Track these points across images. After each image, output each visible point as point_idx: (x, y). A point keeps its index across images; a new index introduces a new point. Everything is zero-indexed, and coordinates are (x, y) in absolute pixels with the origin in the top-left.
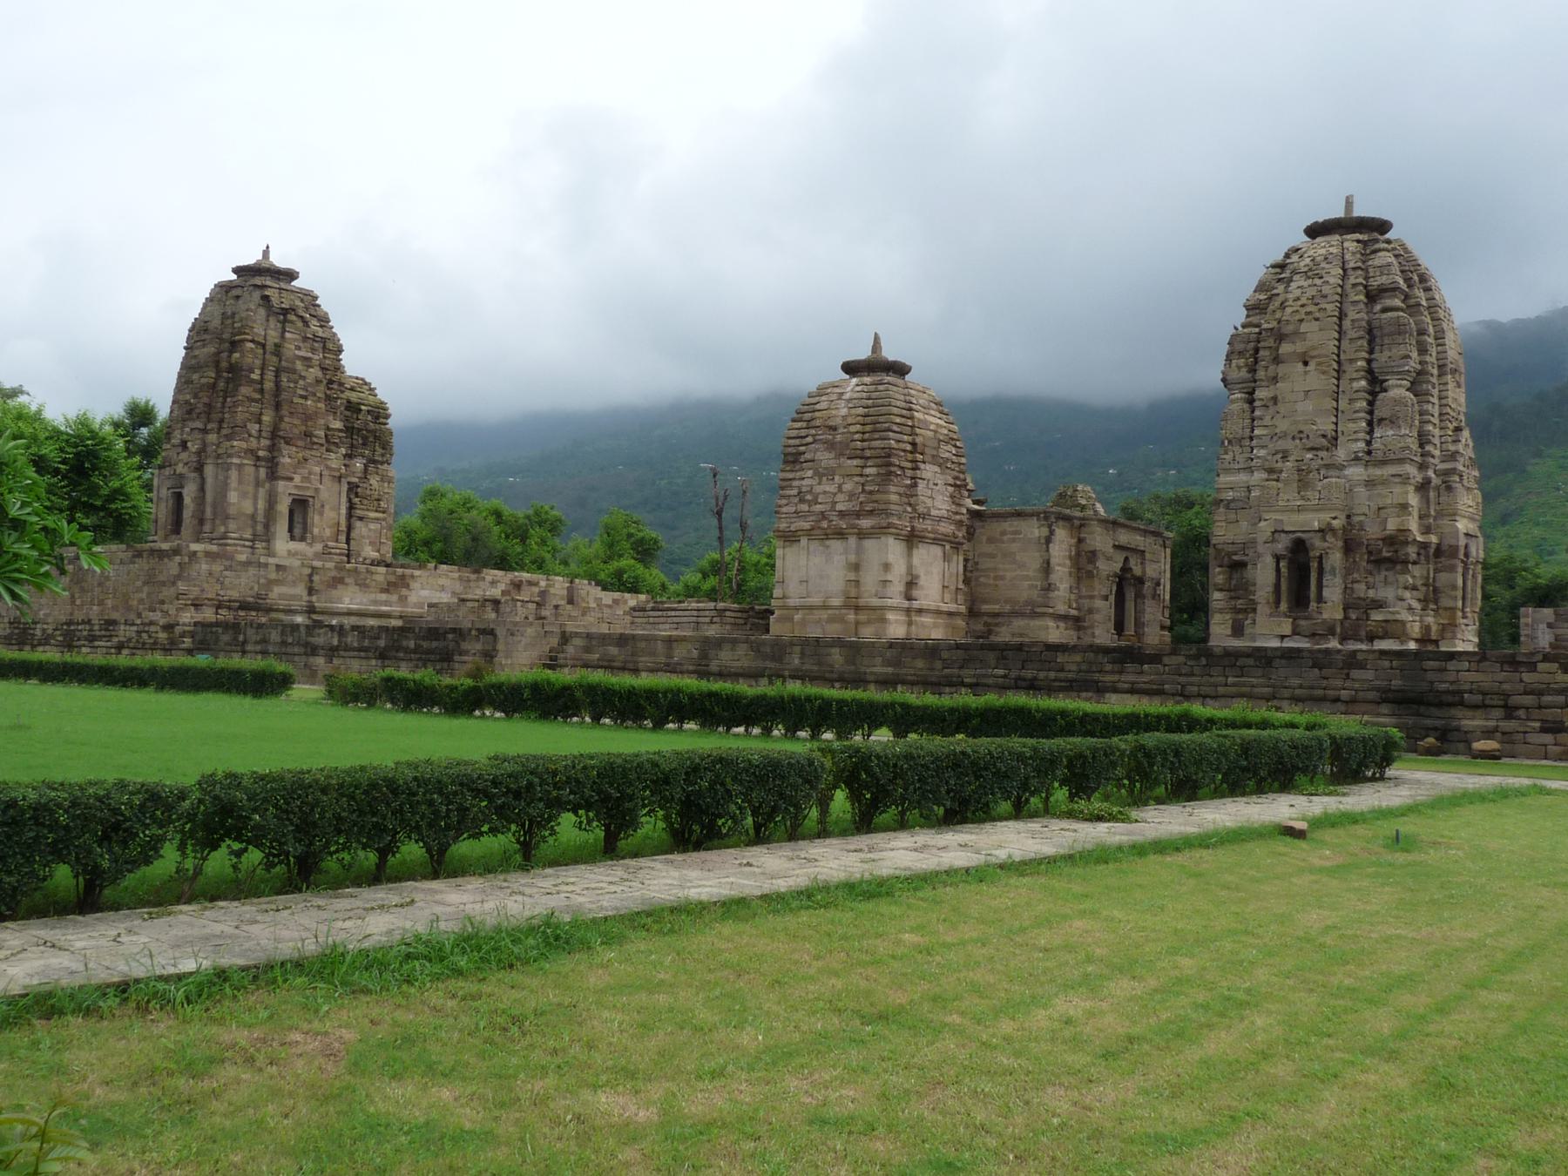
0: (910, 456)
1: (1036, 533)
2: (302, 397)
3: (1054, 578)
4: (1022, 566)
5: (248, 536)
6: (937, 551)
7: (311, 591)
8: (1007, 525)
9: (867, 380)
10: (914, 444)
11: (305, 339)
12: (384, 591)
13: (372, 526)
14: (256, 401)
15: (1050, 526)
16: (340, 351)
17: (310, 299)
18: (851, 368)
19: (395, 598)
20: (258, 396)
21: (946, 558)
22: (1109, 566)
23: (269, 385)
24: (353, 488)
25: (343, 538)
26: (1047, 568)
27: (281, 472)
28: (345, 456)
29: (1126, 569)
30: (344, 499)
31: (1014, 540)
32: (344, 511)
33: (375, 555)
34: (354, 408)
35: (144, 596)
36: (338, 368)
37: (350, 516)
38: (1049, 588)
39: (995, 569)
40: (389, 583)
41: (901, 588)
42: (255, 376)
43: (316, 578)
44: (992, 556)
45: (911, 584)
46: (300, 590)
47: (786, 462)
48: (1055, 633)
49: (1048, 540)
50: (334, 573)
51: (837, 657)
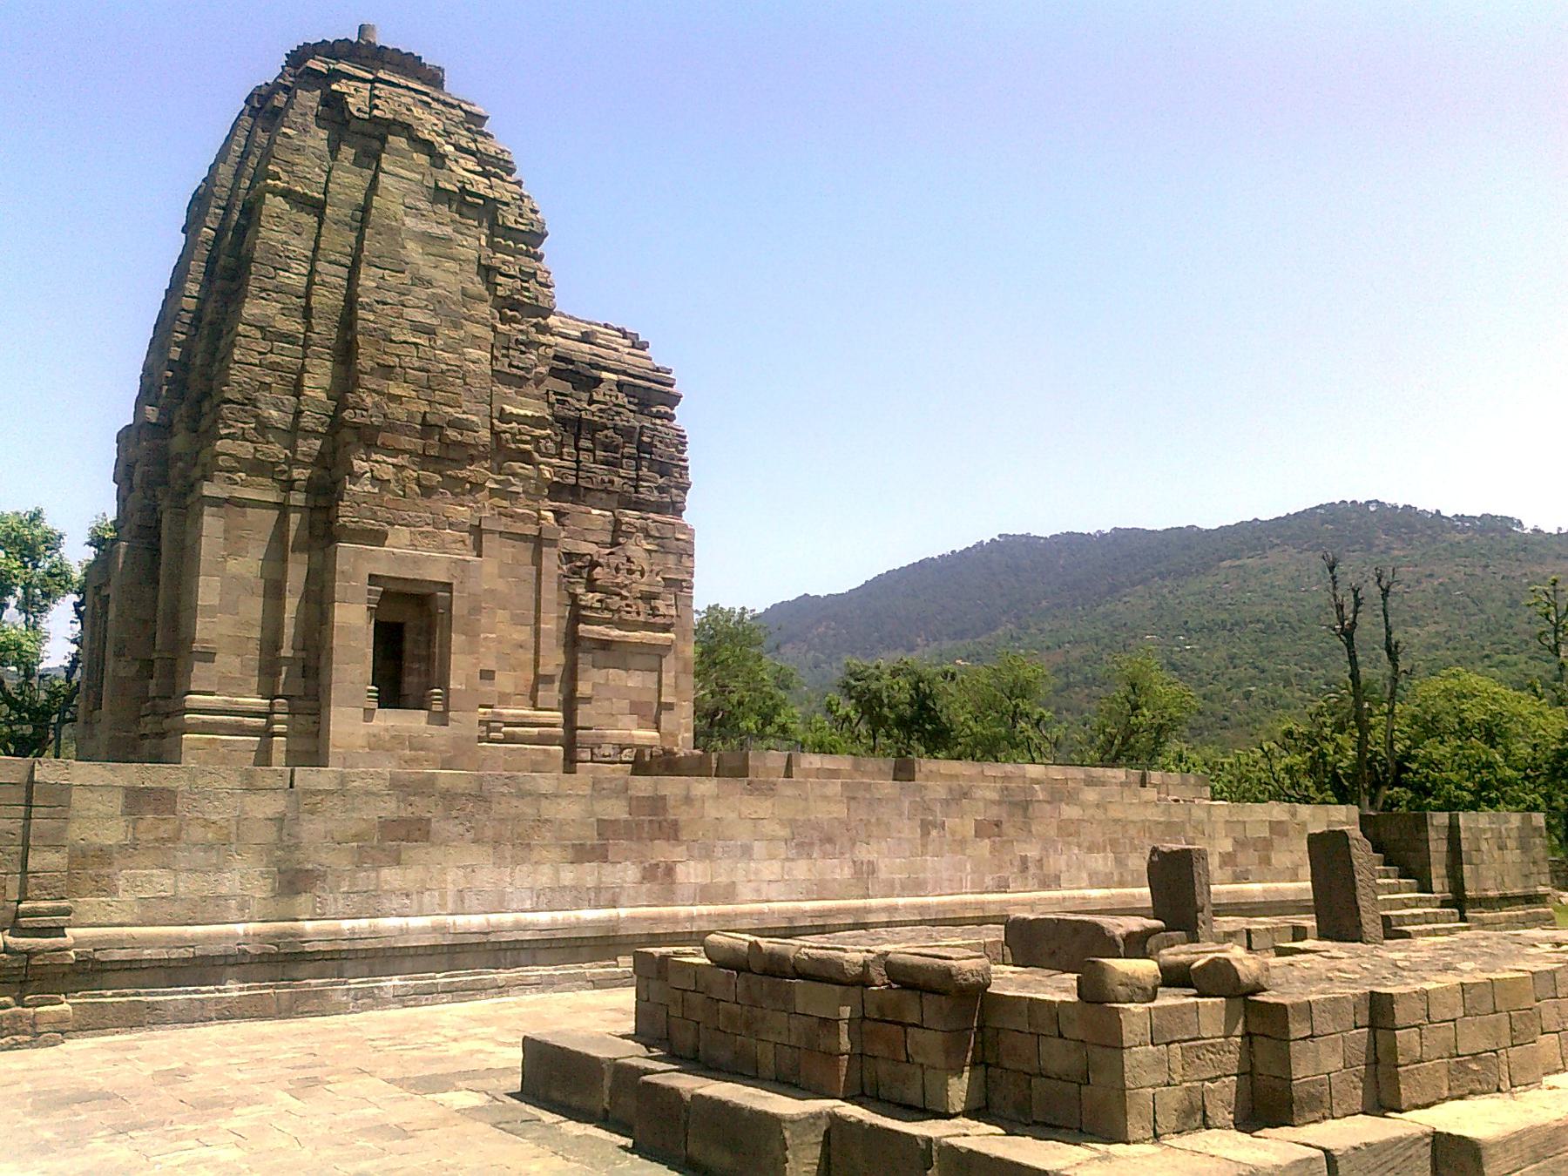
2: (418, 328)
7: (293, 881)
11: (439, 195)
12: (581, 854)
14: (288, 338)
19: (627, 873)
20: (294, 326)
23: (327, 299)
25: (552, 694)
27: (346, 515)
30: (550, 593)
32: (552, 624)
33: (646, 735)
37: (573, 642)
40: (606, 828)
42: (294, 278)
43: (312, 829)
46: (244, 878)
50: (390, 808)
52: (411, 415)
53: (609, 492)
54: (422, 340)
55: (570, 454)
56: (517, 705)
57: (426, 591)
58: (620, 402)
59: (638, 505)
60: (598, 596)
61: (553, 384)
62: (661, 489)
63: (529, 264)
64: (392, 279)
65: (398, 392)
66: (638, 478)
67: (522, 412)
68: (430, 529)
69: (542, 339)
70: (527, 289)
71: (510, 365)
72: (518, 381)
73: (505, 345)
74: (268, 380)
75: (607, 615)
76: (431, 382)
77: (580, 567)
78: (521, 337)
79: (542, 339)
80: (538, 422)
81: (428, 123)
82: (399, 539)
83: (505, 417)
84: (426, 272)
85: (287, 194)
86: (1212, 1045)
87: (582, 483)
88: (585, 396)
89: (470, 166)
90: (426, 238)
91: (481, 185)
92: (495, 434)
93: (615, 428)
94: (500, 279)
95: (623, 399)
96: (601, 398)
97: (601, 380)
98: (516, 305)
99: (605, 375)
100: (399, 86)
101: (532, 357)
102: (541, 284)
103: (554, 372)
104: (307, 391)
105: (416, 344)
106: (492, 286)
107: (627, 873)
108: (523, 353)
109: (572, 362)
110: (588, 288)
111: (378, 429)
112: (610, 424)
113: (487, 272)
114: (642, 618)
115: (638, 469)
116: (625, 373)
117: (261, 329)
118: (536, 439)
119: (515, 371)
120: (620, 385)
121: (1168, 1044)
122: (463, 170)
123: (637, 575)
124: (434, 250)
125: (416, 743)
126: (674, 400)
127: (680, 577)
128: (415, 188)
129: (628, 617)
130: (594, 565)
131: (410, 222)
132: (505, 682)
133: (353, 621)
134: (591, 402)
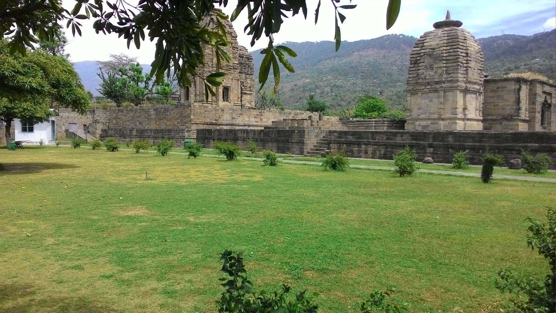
0: (465, 58)
1: (513, 87)
3: (521, 105)
4: (507, 100)
6: (474, 96)
8: (499, 85)
9: (446, 29)
10: (467, 54)
12: (255, 117)
14: (211, 54)
15: (520, 85)
18: (438, 25)
19: (258, 120)
20: (211, 53)
21: (477, 98)
22: (540, 99)
24: (242, 83)
25: (239, 100)
26: (518, 101)
29: (546, 101)
30: (239, 87)
31: (503, 91)
32: (240, 91)
33: (249, 105)
34: (241, 56)
35: (179, 121)
36: (236, 43)
37: (242, 93)
38: (519, 109)
39: (494, 102)
41: (461, 110)
44: (493, 97)
45: (465, 109)
47: (411, 64)
48: (523, 128)
49: (519, 90)
51: (451, 139)
59: (248, 74)
107: (258, 120)
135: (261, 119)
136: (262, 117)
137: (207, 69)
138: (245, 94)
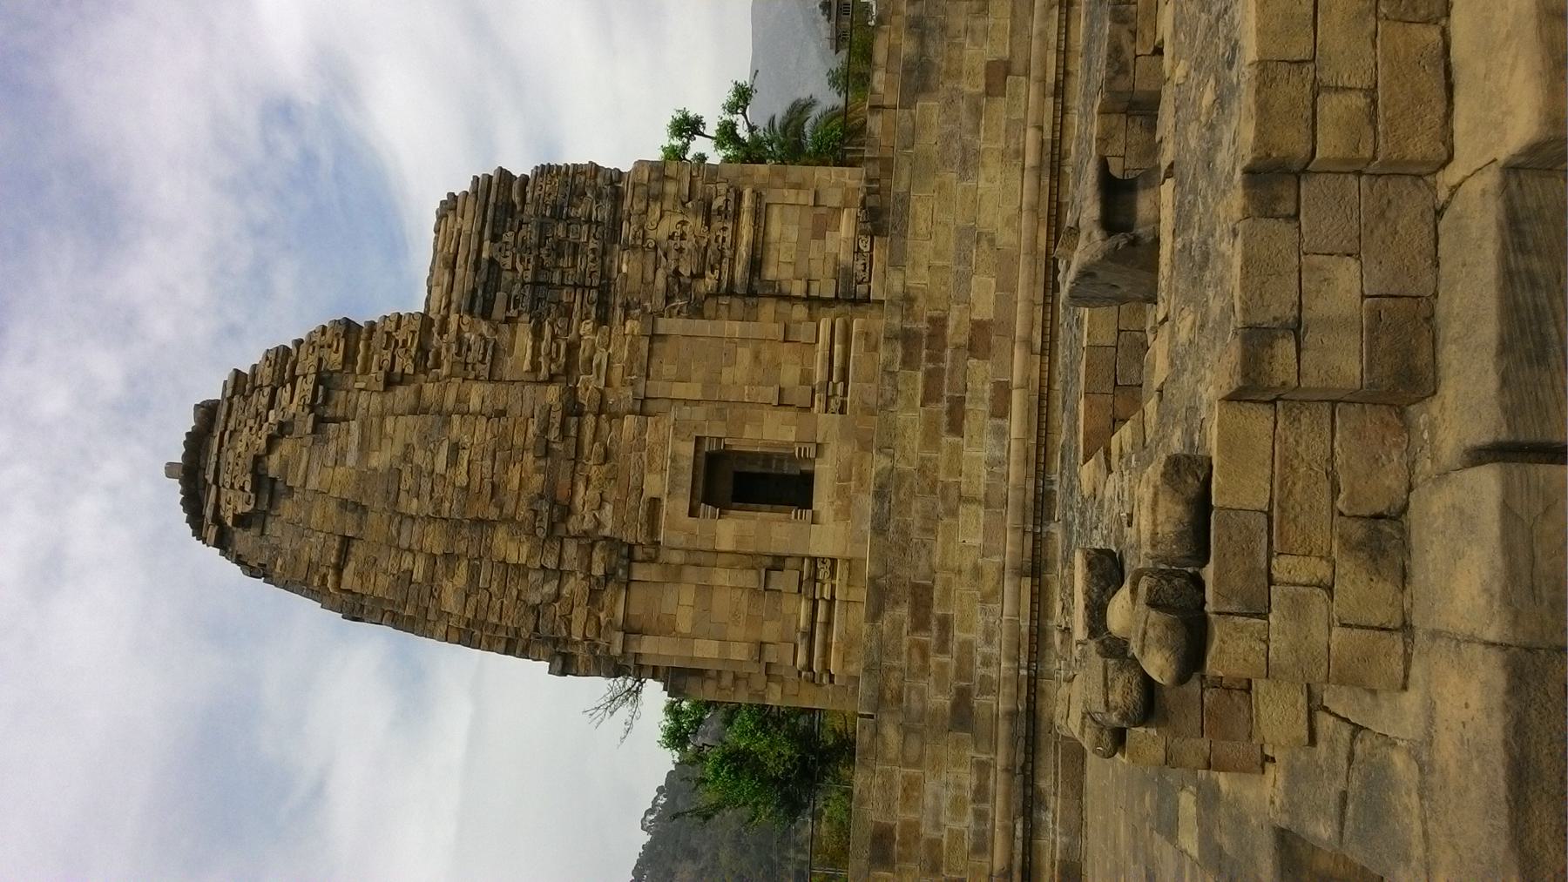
2: (453, 461)
5: (804, 609)
12: (956, 427)
13: (775, 229)
14: (474, 573)
16: (348, 327)
17: (240, 384)
19: (981, 376)
20: (463, 569)
28: (603, 320)
33: (846, 226)
34: (480, 304)
36: (389, 331)
52: (538, 470)
53: (604, 253)
54: (465, 455)
55: (569, 294)
56: (813, 361)
57: (702, 462)
58: (511, 240)
60: (708, 273)
61: (498, 312)
62: (599, 197)
63: (379, 339)
64: (408, 482)
65: (516, 482)
66: (589, 221)
67: (529, 352)
68: (645, 454)
69: (453, 327)
70: (405, 342)
71: (482, 362)
72: (495, 353)
73: (464, 370)
74: (515, 593)
75: (725, 266)
76: (504, 451)
77: (678, 286)
78: (454, 349)
79: (453, 327)
80: (537, 334)
81: (249, 440)
82: (654, 485)
83: (535, 367)
84: (398, 450)
85: (339, 570)
86: (1283, 484)
87: (596, 282)
88: (508, 276)
89: (287, 395)
90: (364, 447)
91: (305, 387)
92: (551, 379)
93: (540, 246)
94: (398, 369)
95: (508, 237)
96: (509, 262)
97: (492, 261)
98: (423, 349)
99: (485, 255)
100: (218, 463)
101: (470, 336)
102: (398, 327)
103: (486, 314)
104: (522, 561)
105: (469, 462)
106: (403, 379)
107: (981, 376)
108: (469, 349)
109: (474, 291)
110: (401, 280)
111: (554, 502)
112: (535, 253)
113: (390, 382)
114: (729, 225)
115: (578, 220)
116: (481, 233)
117: (467, 596)
118: (554, 337)
119: (488, 358)
120: (495, 238)
121: (1271, 582)
122: (293, 402)
123: (687, 229)
124: (375, 440)
125: (844, 477)
126: (504, 175)
127: (687, 179)
128: (316, 456)
129: (728, 240)
130: (677, 273)
131: (351, 460)
132: (790, 376)
133: (730, 530)
134: (514, 269)
135: (980, 340)
136: (957, 331)
137: (579, 615)
138: (756, 264)
